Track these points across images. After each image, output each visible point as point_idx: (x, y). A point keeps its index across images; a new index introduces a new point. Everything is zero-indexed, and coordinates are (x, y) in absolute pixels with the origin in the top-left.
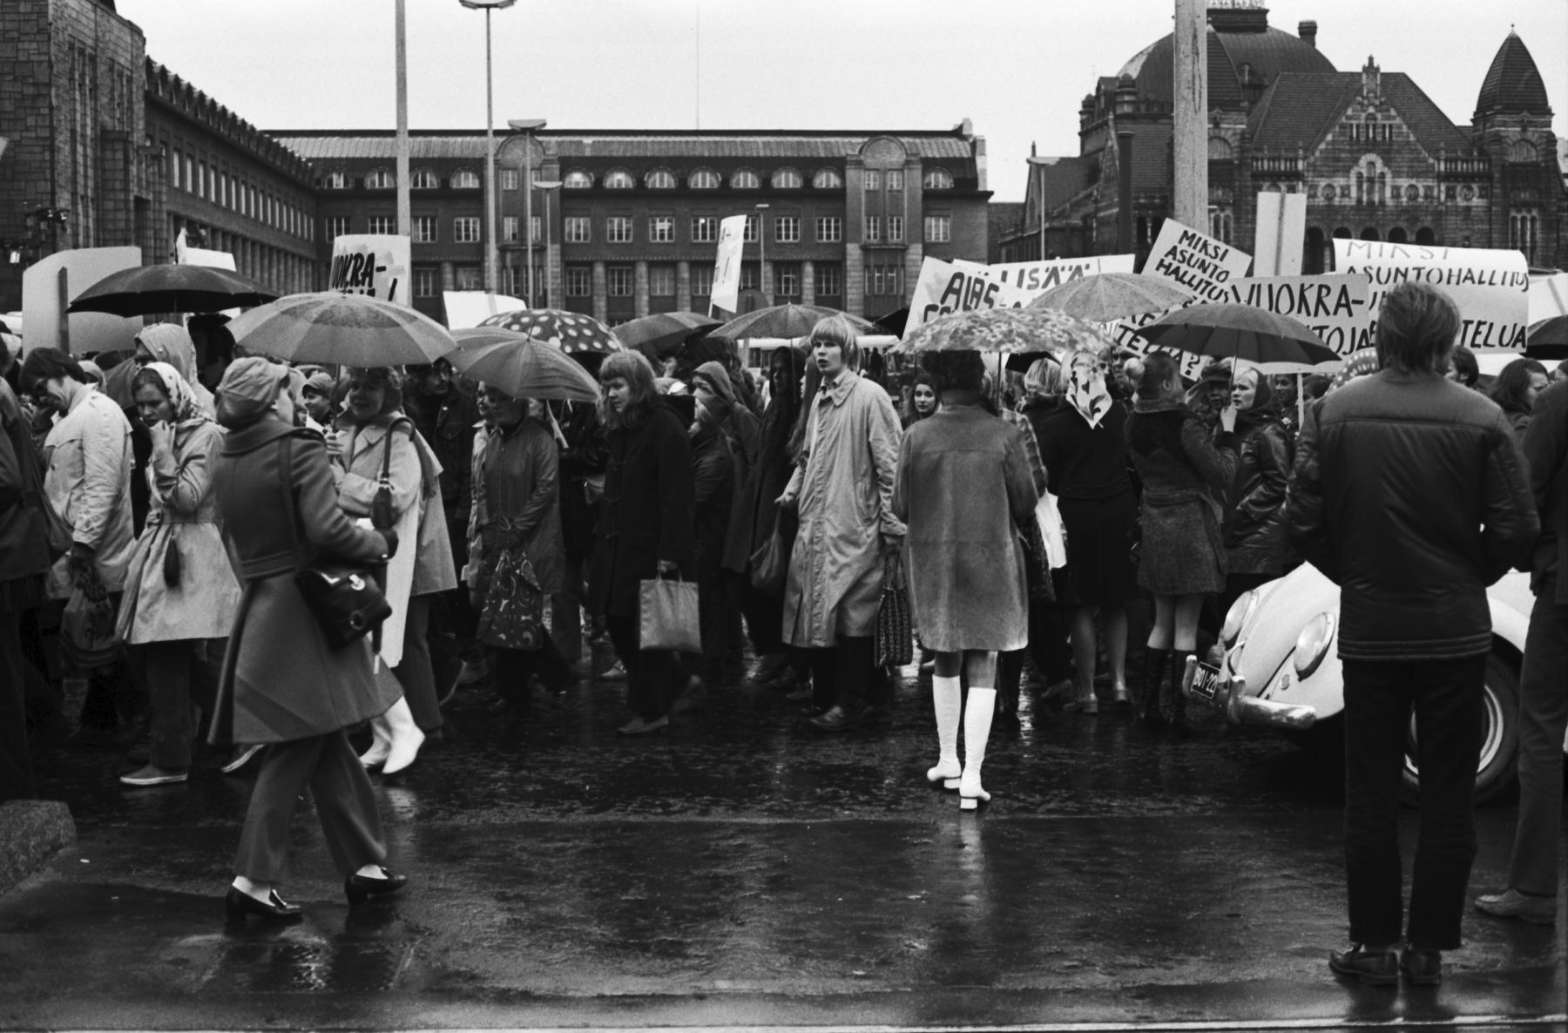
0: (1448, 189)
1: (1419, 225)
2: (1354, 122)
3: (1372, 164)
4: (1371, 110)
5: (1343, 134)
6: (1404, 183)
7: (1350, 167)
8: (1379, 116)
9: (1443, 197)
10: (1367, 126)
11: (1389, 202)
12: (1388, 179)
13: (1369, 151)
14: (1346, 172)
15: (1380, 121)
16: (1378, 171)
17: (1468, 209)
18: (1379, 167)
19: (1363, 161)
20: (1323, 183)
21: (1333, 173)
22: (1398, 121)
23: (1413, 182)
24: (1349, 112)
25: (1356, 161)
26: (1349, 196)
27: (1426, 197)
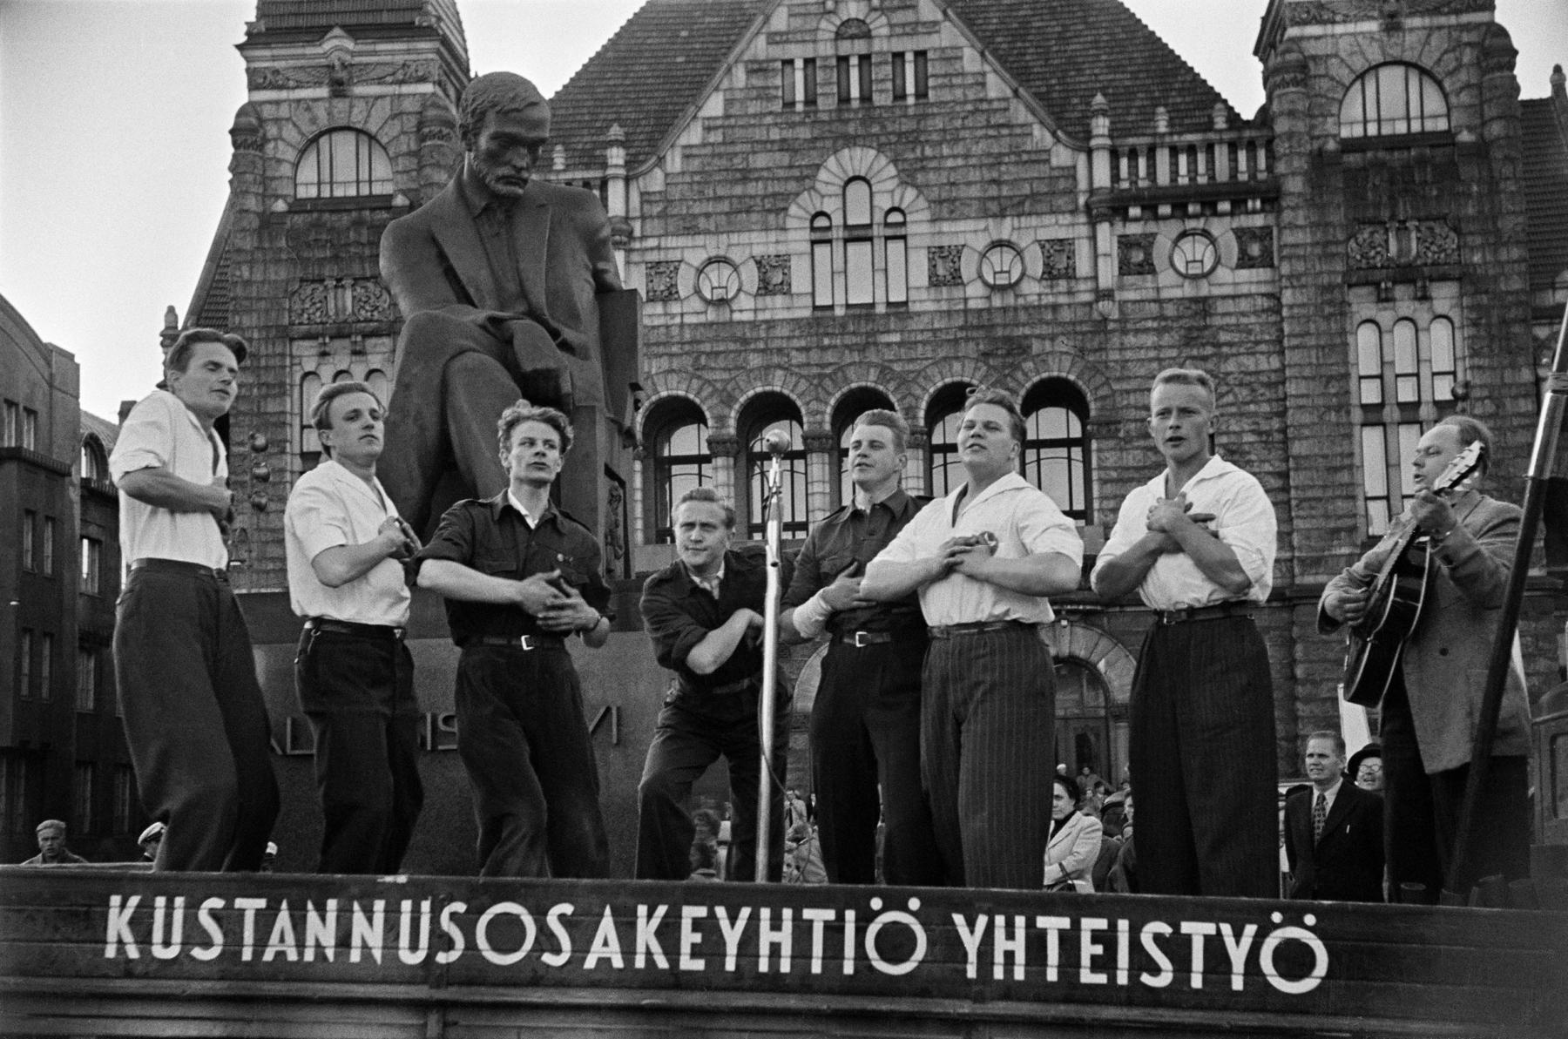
0: (1126, 243)
5: (764, 95)
6: (971, 233)
7: (789, 197)
8: (879, 26)
9: (1108, 274)
10: (843, 60)
11: (924, 302)
13: (850, 141)
16: (884, 202)
17: (1203, 305)
19: (831, 172)
20: (693, 251)
21: (739, 214)
22: (950, 35)
24: (780, 21)
25: (806, 178)
26: (785, 289)
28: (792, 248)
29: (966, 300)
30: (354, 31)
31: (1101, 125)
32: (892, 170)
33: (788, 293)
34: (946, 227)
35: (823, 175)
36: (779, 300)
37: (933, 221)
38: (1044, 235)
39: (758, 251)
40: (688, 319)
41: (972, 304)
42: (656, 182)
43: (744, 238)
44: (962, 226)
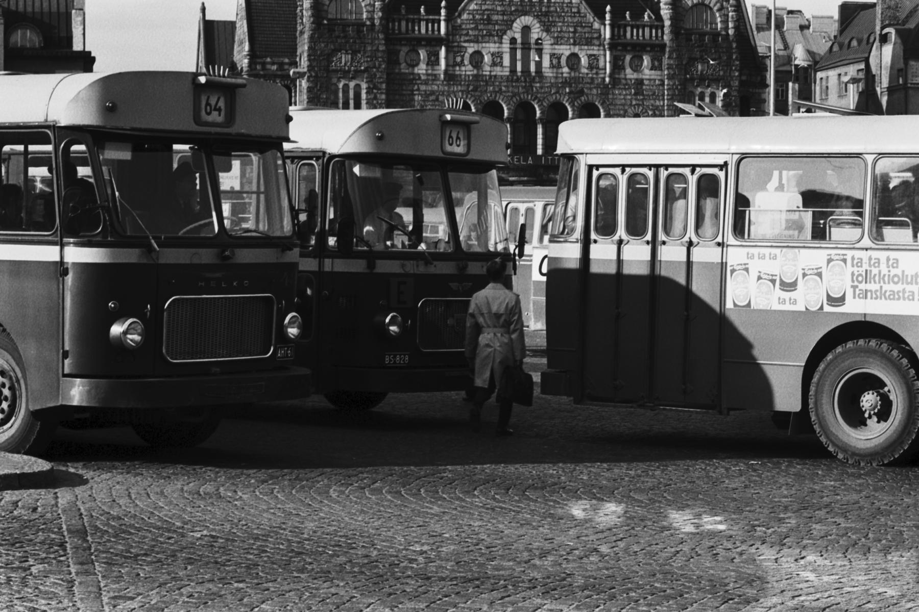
3: (526, 30)
6: (565, 51)
12: (547, 48)
13: (525, 13)
18: (536, 33)
19: (517, 26)
23: (576, 49)
25: (509, 25)
27: (591, 67)
28: (504, 50)
29: (562, 73)
32: (538, 25)
33: (502, 66)
34: (556, 47)
35: (515, 25)
36: (498, 68)
37: (552, 45)
38: (590, 52)
39: (492, 50)
40: (468, 73)
41: (565, 75)
43: (487, 45)
44: (562, 47)
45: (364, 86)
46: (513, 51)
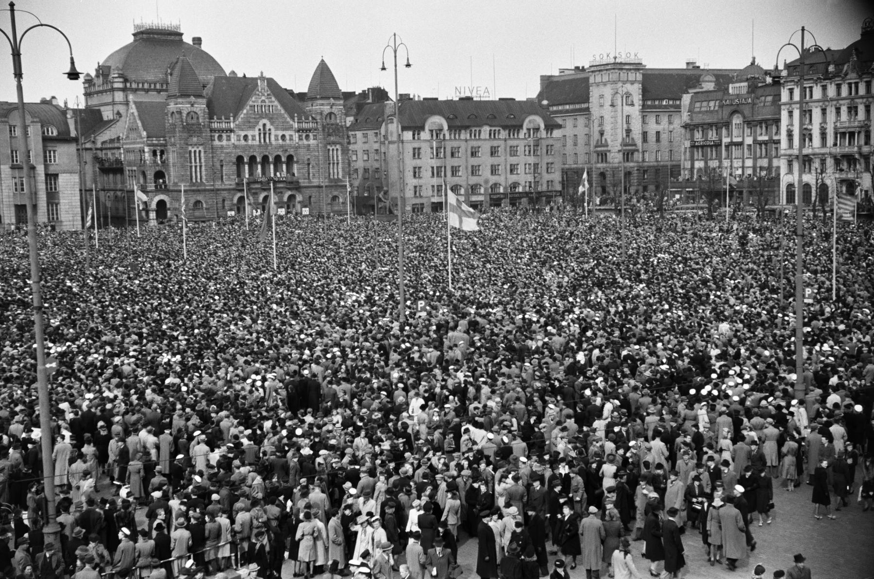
0: (300, 136)
1: (287, 154)
2: (256, 104)
3: (264, 125)
4: (263, 98)
6: (280, 133)
8: (267, 101)
12: (273, 132)
14: (252, 127)
15: (267, 104)
17: (309, 145)
23: (284, 133)
24: (253, 99)
25: (258, 123)
30: (194, 96)
31: (296, 119)
42: (237, 123)
45: (202, 151)
46: (260, 134)
